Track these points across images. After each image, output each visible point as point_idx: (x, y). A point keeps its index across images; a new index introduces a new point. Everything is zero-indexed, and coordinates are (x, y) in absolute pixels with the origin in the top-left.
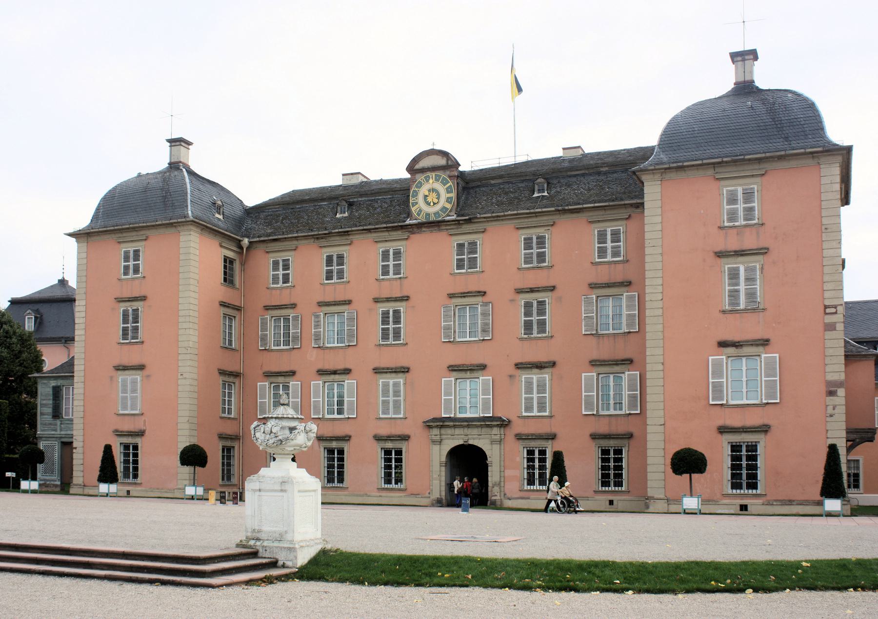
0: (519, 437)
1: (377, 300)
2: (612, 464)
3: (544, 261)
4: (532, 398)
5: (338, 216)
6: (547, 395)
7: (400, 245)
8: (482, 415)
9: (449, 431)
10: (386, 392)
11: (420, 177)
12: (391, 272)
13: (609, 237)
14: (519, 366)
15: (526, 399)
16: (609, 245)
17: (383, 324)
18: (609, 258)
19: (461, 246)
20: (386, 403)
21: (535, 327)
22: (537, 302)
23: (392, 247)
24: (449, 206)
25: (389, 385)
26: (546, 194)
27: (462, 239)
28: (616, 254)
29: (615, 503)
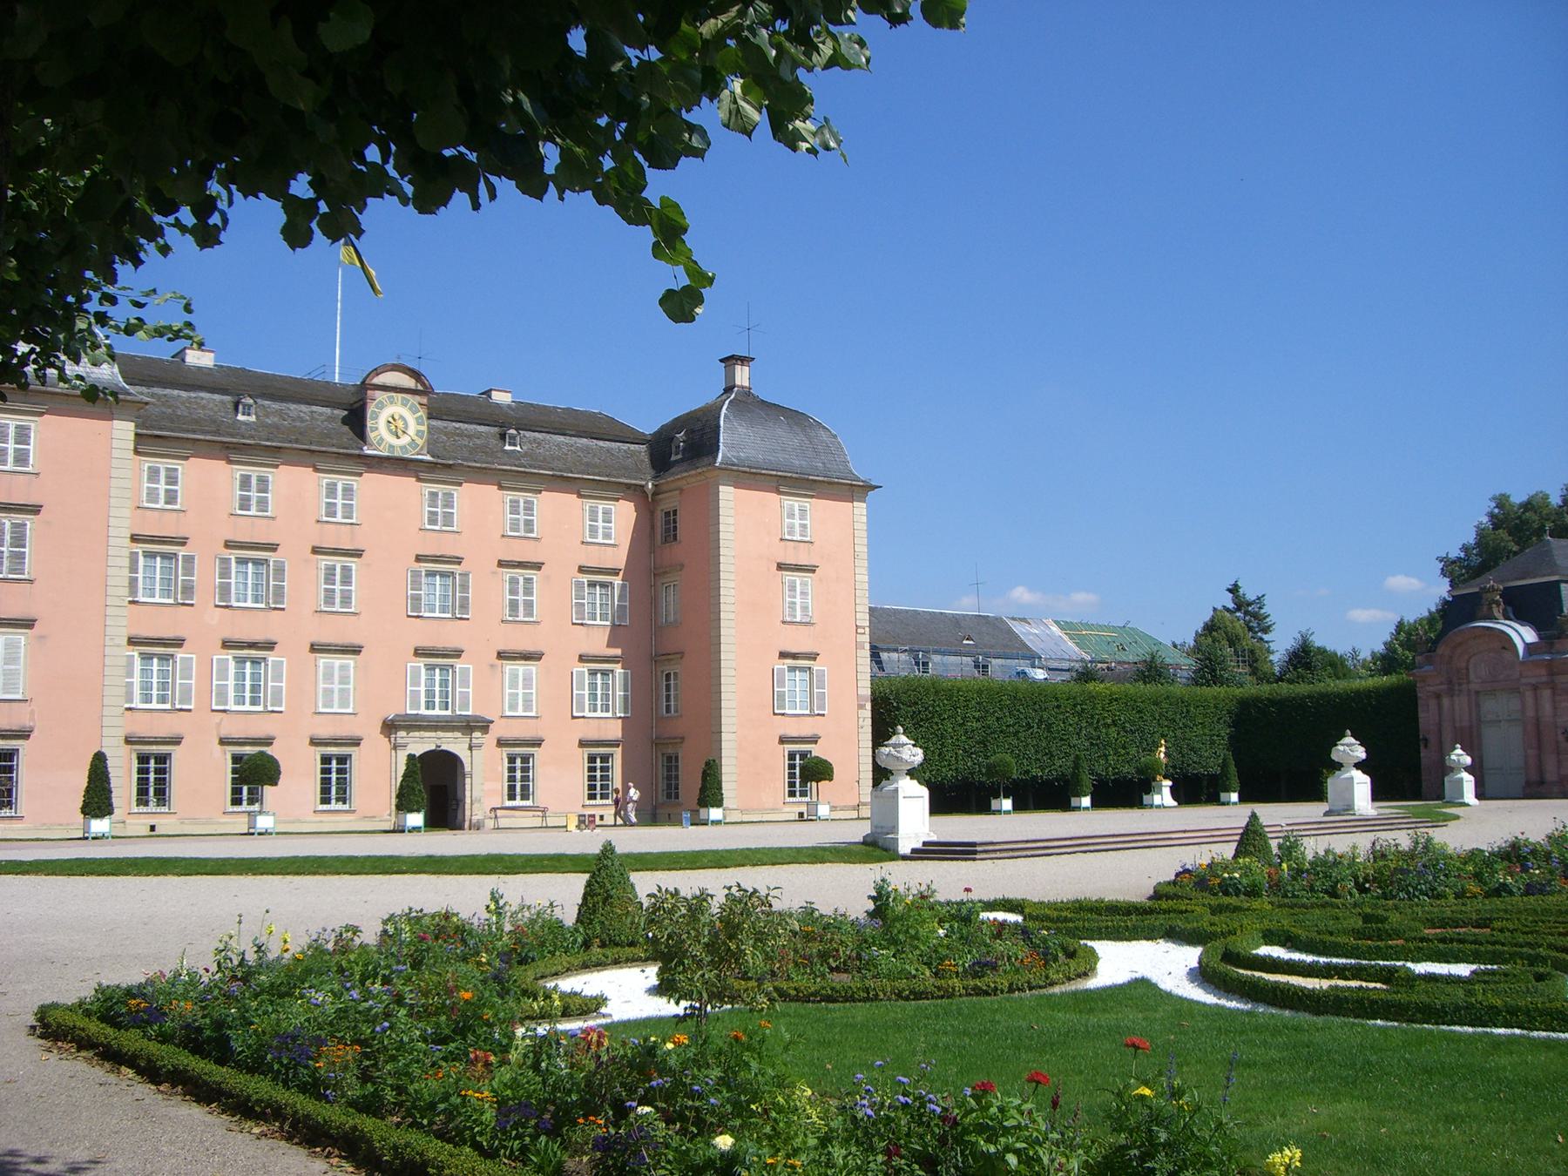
0: (501, 743)
1: (316, 550)
2: (598, 774)
3: (532, 531)
4: (517, 694)
5: (240, 417)
6: (534, 691)
7: (354, 482)
8: (458, 713)
9: (417, 734)
10: (329, 676)
11: (381, 396)
12: (339, 514)
13: (600, 515)
14: (501, 655)
15: (510, 694)
16: (600, 524)
17: (325, 583)
18: (600, 540)
19: (434, 495)
20: (328, 692)
21: (521, 608)
22: (525, 579)
23: (341, 481)
24: (420, 442)
25: (333, 667)
26: (518, 448)
27: (435, 487)
28: (607, 536)
29: (605, 818)
